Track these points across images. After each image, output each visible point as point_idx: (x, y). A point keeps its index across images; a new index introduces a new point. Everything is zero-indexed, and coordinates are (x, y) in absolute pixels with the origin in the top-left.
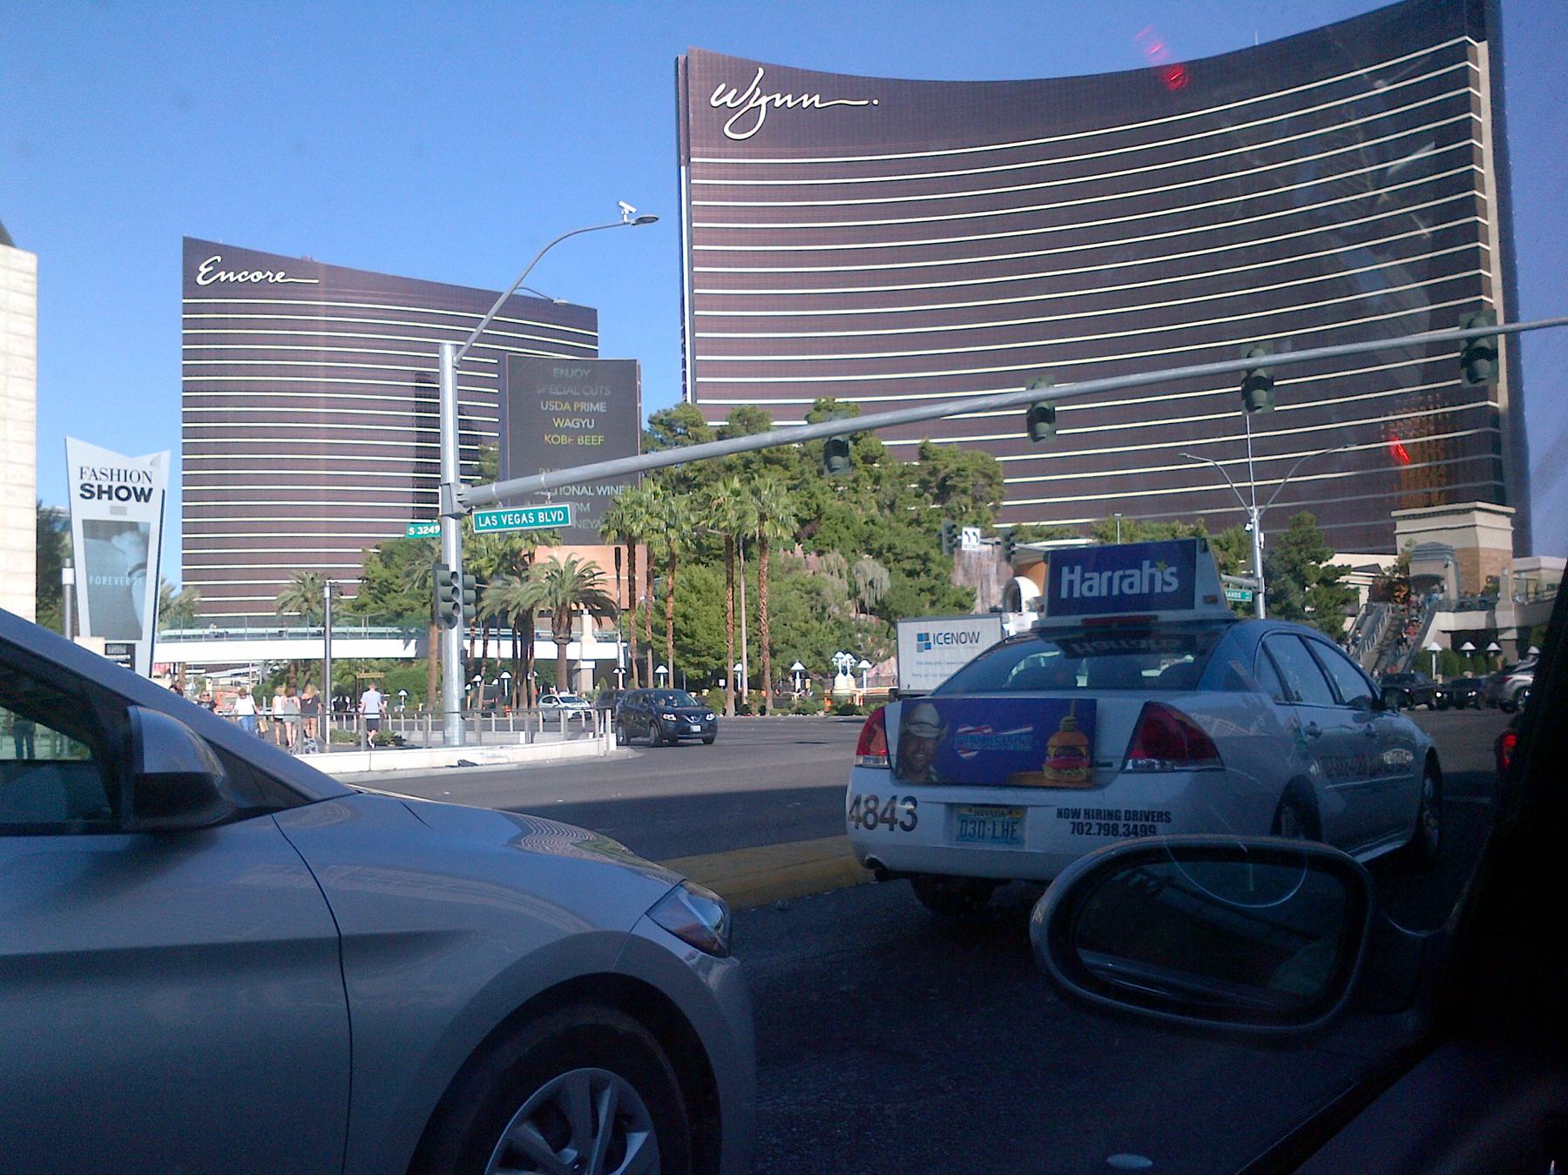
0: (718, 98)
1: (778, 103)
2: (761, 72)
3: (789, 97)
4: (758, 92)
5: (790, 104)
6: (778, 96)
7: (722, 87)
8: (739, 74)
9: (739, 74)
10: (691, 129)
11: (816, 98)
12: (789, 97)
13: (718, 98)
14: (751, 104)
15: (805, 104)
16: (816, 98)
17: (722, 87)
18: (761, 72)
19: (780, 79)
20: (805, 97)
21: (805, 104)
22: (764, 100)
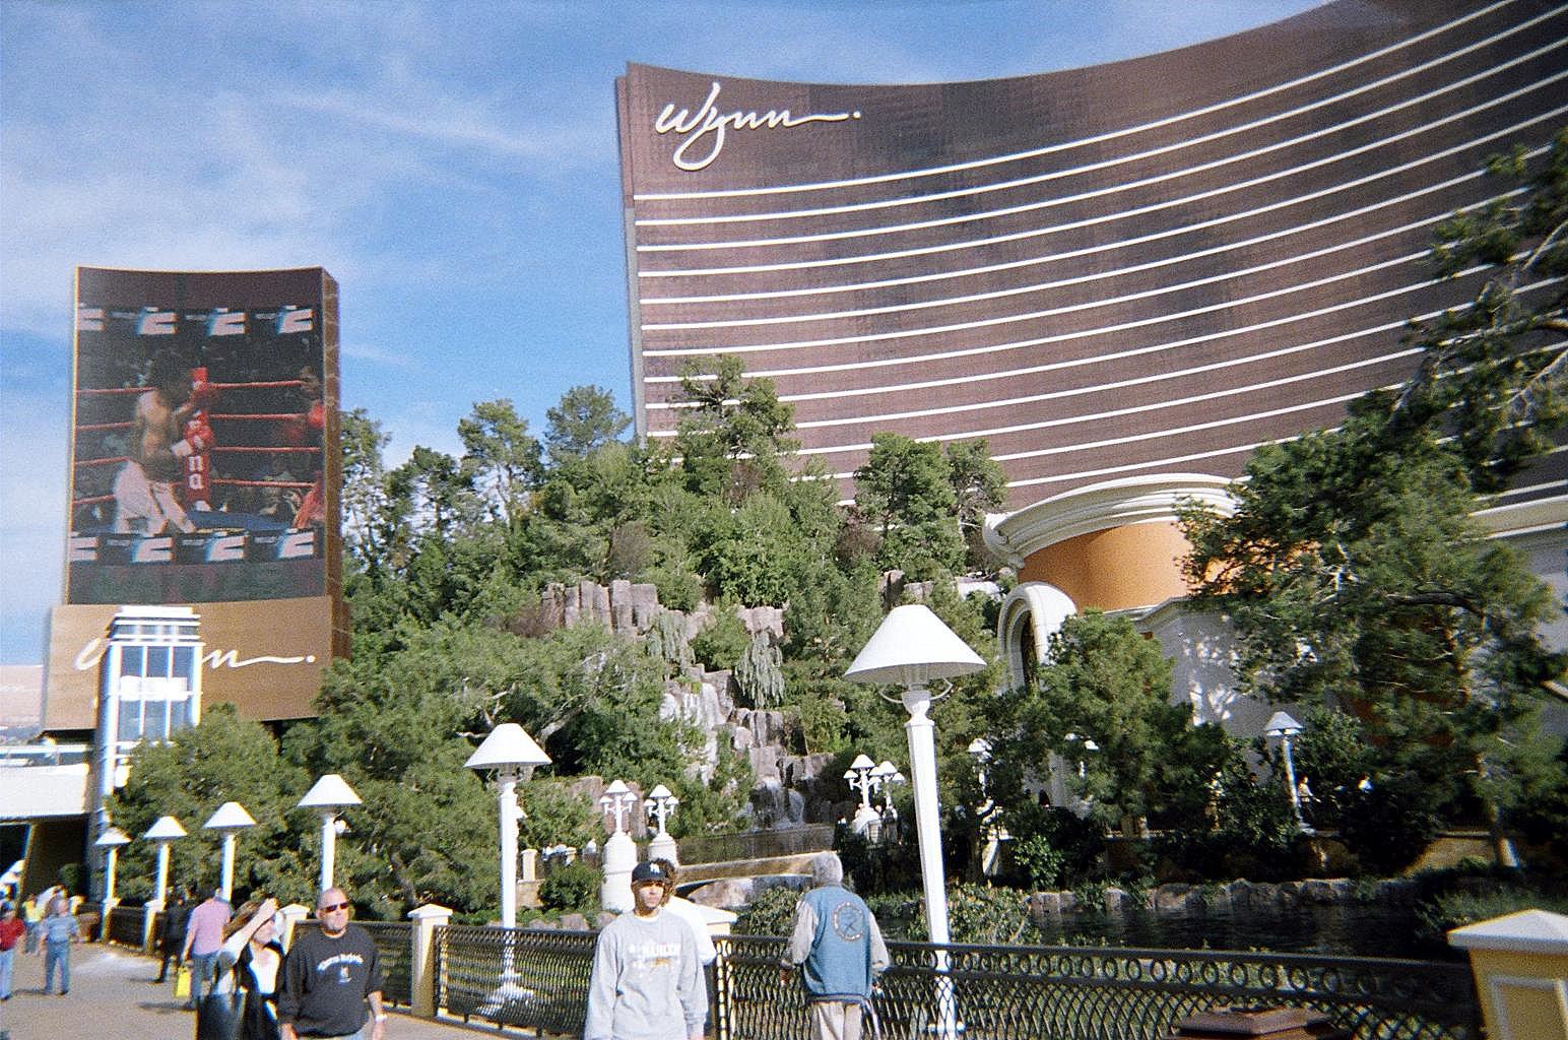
0: (665, 123)
1: (738, 125)
2: (716, 88)
3: (752, 116)
4: (714, 111)
5: (753, 125)
6: (738, 115)
7: (670, 108)
8: (687, 89)
9: (687, 89)
10: (641, 159)
11: (786, 115)
12: (752, 116)
13: (665, 123)
14: (706, 127)
15: (772, 124)
16: (786, 115)
17: (670, 108)
18: (716, 88)
19: (740, 94)
20: (772, 114)
21: (772, 124)
22: (723, 120)
